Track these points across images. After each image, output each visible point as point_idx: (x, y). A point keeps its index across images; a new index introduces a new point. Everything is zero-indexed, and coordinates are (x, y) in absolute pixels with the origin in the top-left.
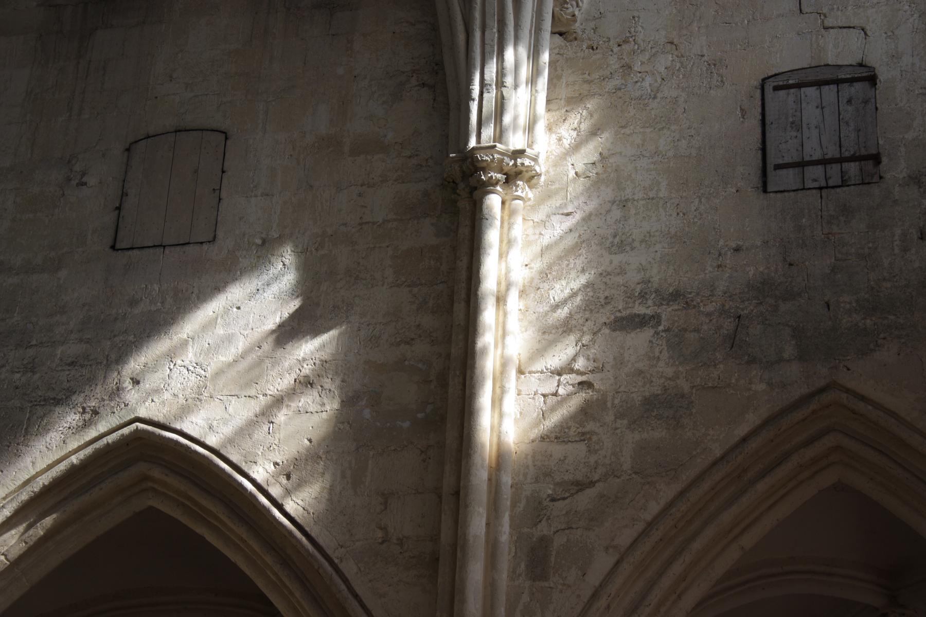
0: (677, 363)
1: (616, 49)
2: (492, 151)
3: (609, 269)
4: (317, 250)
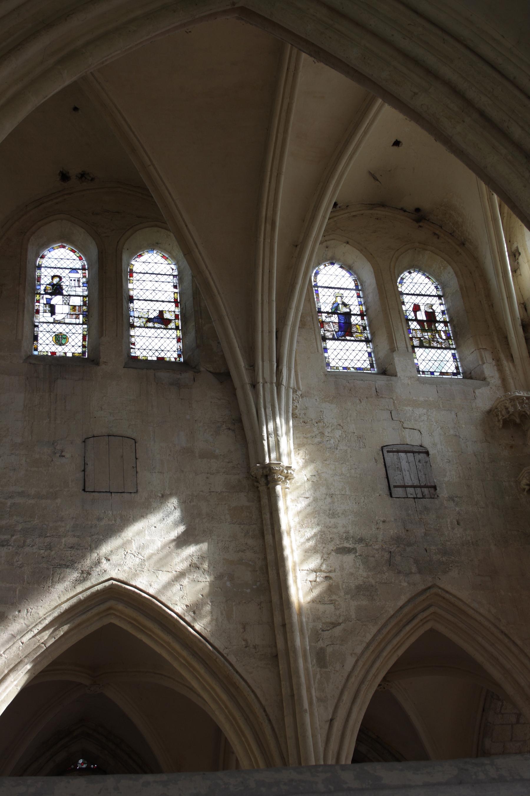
0: (367, 571)
1: (316, 425)
2: (279, 465)
3: (330, 525)
4: (190, 502)
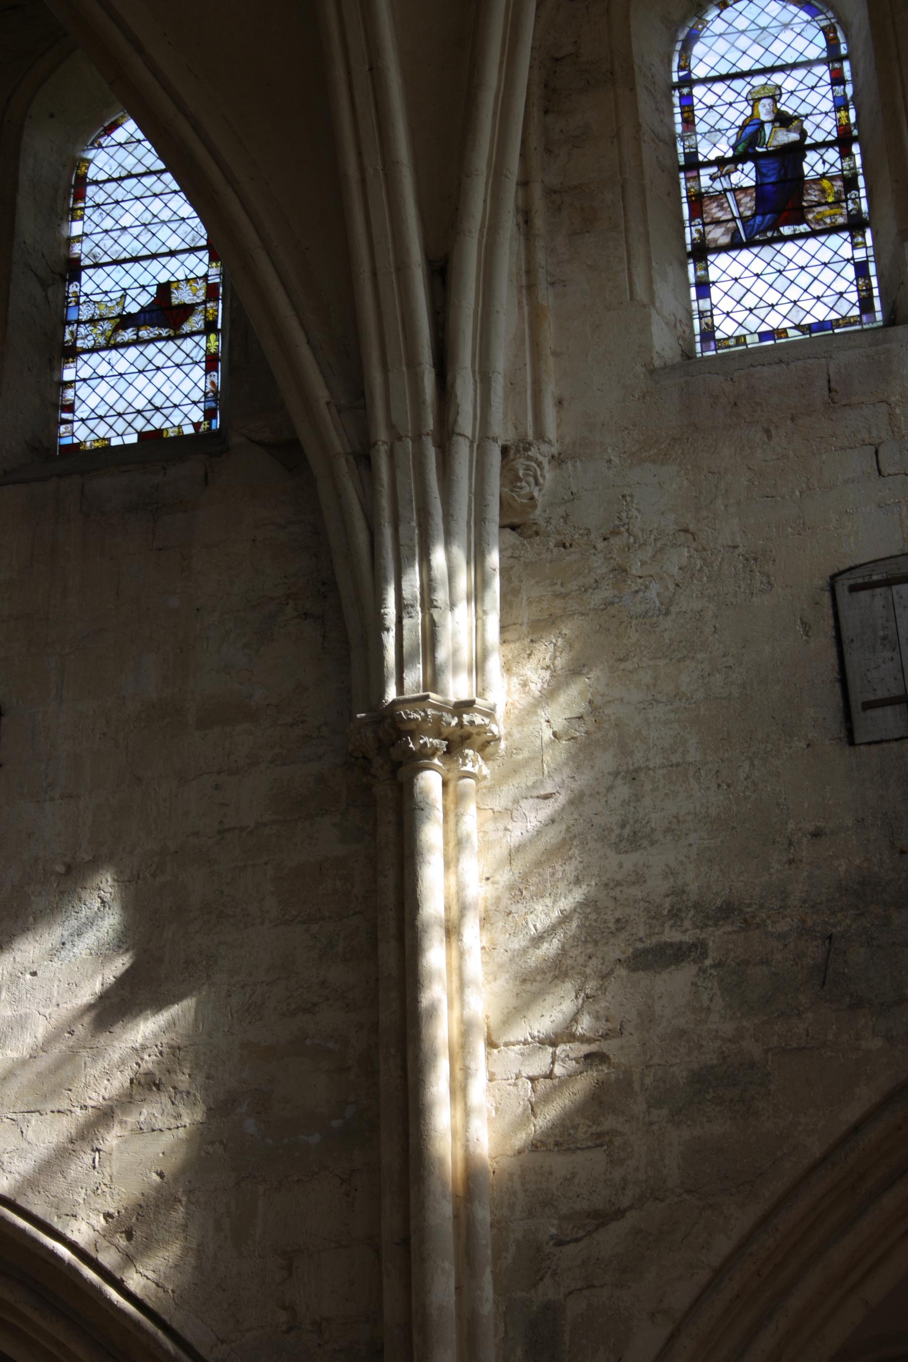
0: (739, 1015)
1: (601, 545)
2: (423, 704)
3: (619, 877)
4: (154, 876)
